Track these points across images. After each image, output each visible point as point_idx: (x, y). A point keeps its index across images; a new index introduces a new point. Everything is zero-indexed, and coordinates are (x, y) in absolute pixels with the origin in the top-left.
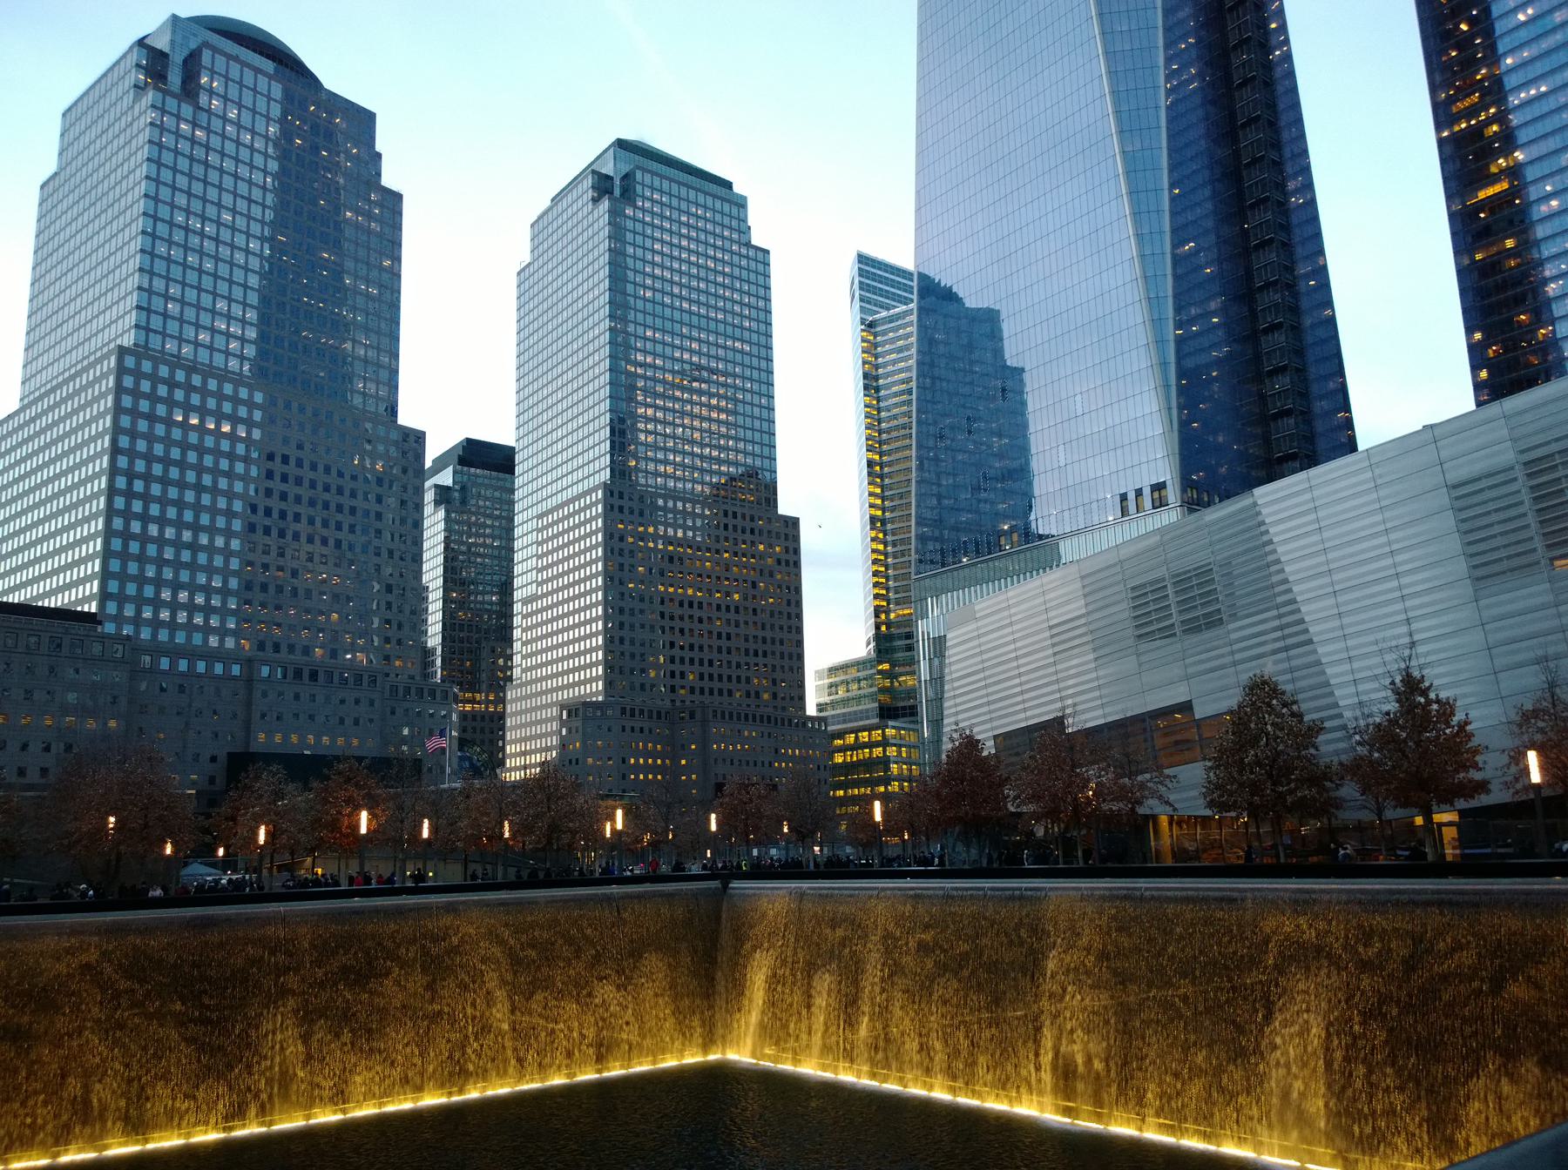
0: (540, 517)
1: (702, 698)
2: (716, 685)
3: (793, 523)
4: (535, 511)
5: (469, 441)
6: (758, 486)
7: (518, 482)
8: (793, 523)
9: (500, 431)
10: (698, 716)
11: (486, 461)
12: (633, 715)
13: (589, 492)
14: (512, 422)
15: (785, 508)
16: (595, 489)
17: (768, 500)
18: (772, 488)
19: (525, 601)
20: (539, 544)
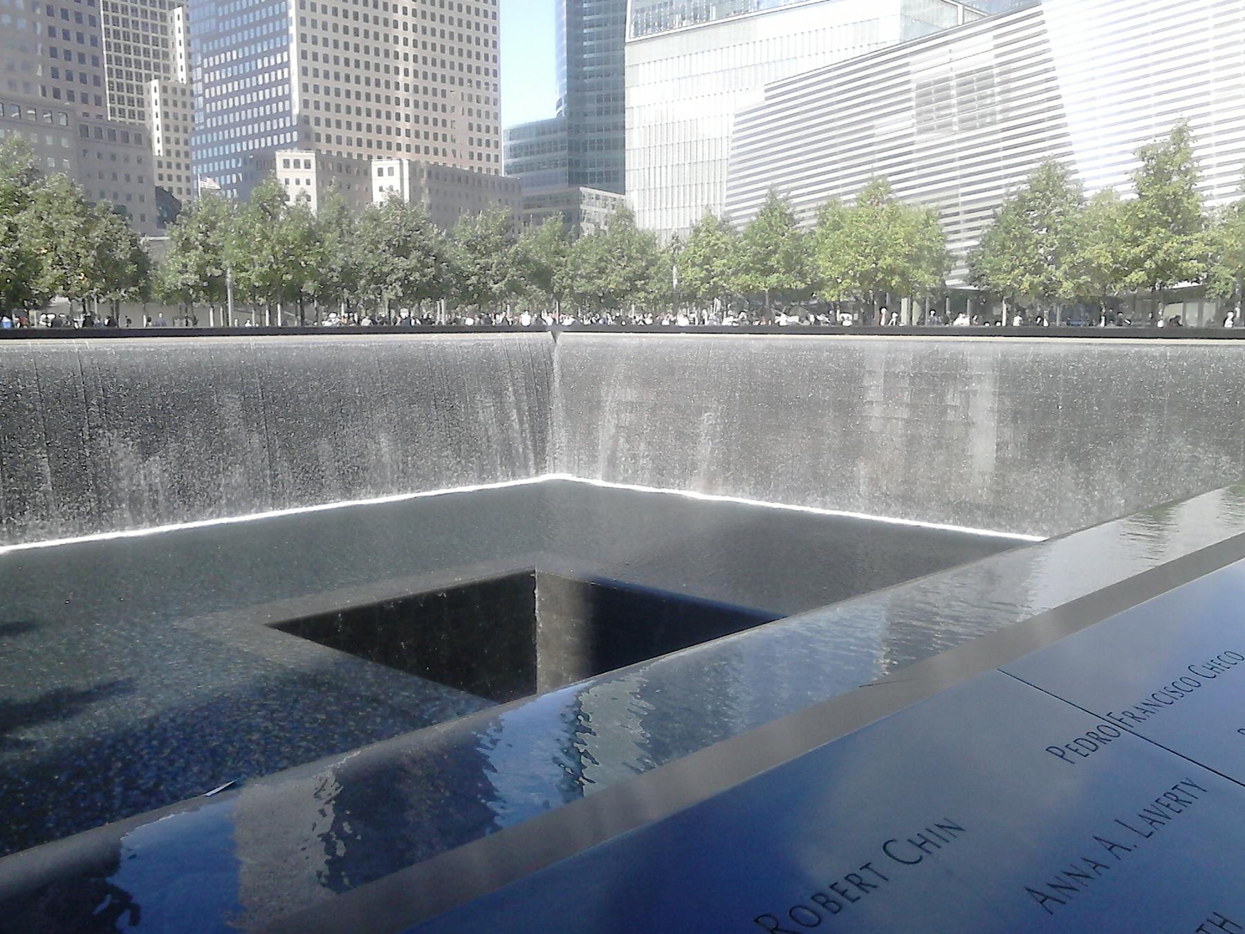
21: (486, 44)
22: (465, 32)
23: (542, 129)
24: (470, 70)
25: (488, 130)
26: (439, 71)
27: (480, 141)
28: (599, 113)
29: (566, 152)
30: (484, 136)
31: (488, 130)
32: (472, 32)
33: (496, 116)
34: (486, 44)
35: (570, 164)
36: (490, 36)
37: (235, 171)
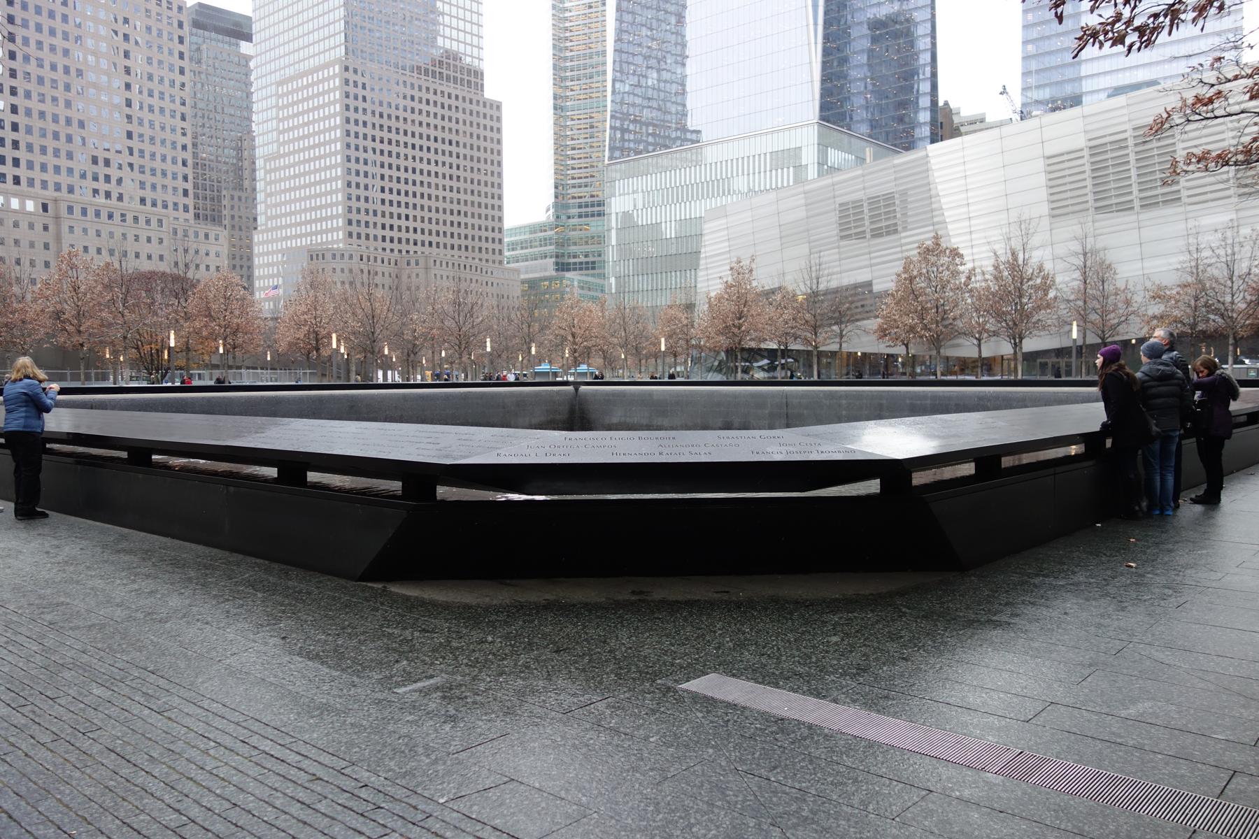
0: (280, 84)
1: (423, 249)
2: (441, 239)
3: (499, 107)
13: (326, 66)
15: (490, 93)
18: (478, 74)
19: (268, 159)
22: (476, 154)
23: (534, 229)
24: (479, 183)
25: (493, 230)
26: (455, 184)
27: (487, 239)
28: (580, 216)
29: (553, 247)
30: (490, 235)
31: (493, 230)
32: (482, 155)
33: (500, 219)
35: (557, 257)
36: (495, 157)
37: (277, 264)
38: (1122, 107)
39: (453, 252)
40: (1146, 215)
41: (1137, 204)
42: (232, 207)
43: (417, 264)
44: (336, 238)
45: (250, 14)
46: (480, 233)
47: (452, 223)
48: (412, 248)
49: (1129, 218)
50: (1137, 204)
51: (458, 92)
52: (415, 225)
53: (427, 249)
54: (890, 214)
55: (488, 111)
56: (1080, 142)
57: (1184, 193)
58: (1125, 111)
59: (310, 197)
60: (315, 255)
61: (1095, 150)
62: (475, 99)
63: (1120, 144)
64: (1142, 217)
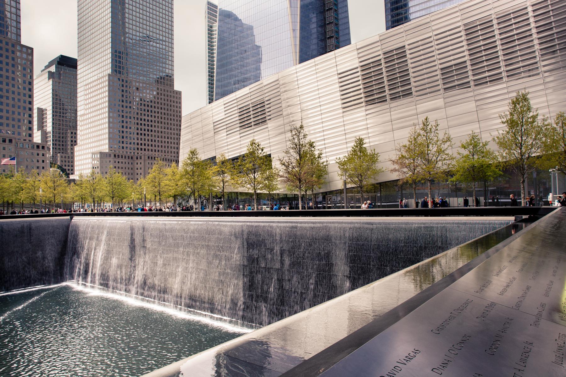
0: (86, 85)
3: (179, 93)
4: (85, 83)
5: (61, 56)
6: (167, 80)
7: (79, 72)
8: (179, 93)
9: (72, 54)
10: (143, 158)
11: (66, 65)
12: (119, 157)
14: (76, 50)
15: (176, 88)
16: (105, 76)
17: (170, 85)
18: (172, 81)
19: (81, 116)
20: (85, 95)
21: (177, 116)
34: (177, 116)
38: (378, 42)
39: (158, 153)
40: (395, 104)
41: (388, 98)
42: (72, 137)
43: (141, 158)
44: (105, 148)
45: (76, 57)
46: (171, 145)
47: (165, 142)
48: (140, 152)
49: (385, 106)
50: (388, 98)
51: (162, 87)
52: (141, 142)
53: (143, 152)
54: (263, 112)
55: (175, 95)
56: (356, 63)
57: (414, 90)
58: (379, 44)
59: (100, 130)
60: (102, 155)
61: (364, 68)
62: (169, 90)
63: (378, 63)
64: (392, 105)
